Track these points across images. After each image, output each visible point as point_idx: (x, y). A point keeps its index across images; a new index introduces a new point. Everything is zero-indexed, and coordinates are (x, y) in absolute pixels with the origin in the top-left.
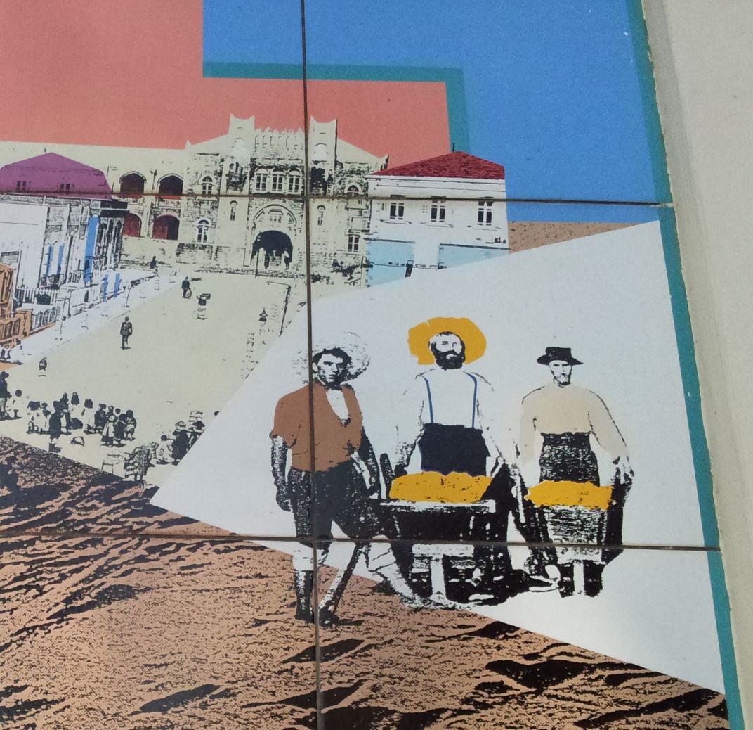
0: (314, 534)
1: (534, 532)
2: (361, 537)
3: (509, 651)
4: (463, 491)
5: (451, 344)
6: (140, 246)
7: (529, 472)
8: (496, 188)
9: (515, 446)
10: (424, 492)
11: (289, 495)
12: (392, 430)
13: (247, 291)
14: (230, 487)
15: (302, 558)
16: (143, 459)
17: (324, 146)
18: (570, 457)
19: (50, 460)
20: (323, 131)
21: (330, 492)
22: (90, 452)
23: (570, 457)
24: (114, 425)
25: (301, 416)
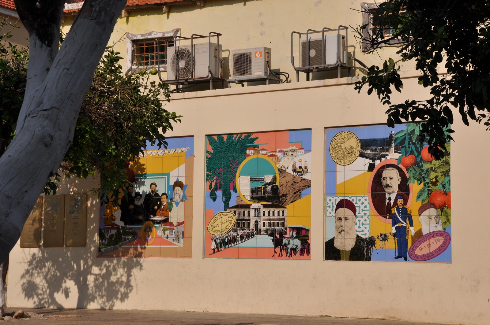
0: (294, 173)
1: (304, 172)
2: (296, 173)
3: (302, 179)
4: (300, 170)
5: (300, 161)
6: (285, 155)
7: (304, 169)
8: (303, 150)
9: (303, 167)
10: (299, 170)
11: (293, 171)
12: (297, 167)
13: (291, 158)
14: (290, 170)
15: (293, 174)
16: (286, 169)
17: (295, 148)
18: (306, 168)
19: (281, 169)
20: (295, 146)
21: (294, 171)
22: (283, 169)
23: (306, 168)
24: (284, 167)
25: (294, 166)
